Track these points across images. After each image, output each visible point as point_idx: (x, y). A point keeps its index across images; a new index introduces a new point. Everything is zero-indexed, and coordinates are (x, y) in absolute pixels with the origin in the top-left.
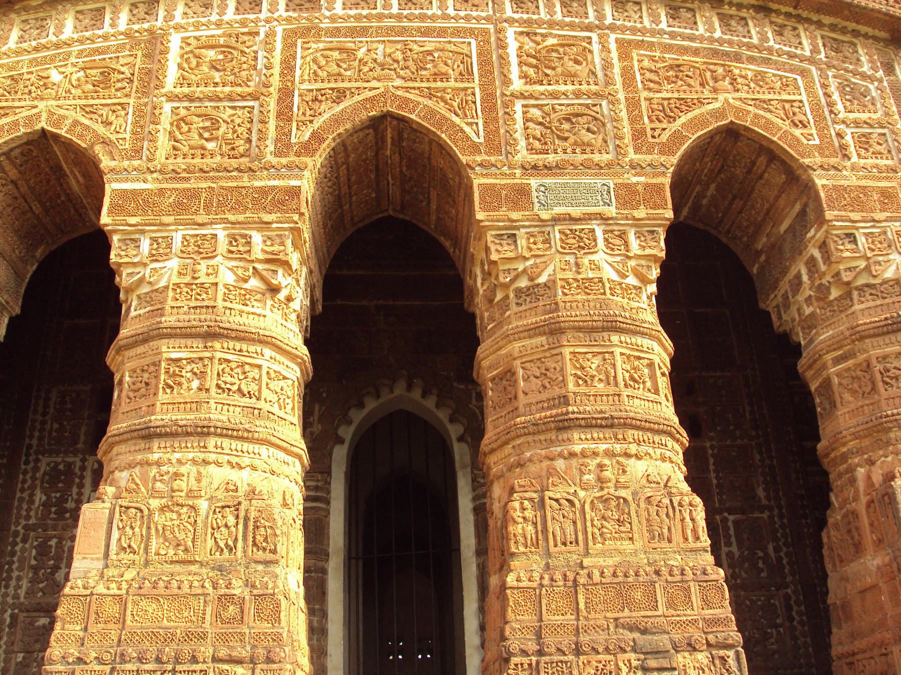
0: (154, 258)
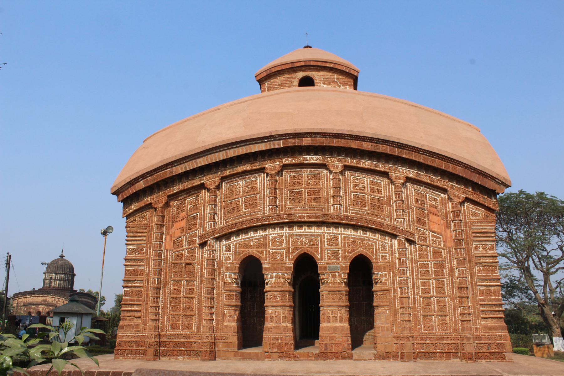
0: (271, 278)
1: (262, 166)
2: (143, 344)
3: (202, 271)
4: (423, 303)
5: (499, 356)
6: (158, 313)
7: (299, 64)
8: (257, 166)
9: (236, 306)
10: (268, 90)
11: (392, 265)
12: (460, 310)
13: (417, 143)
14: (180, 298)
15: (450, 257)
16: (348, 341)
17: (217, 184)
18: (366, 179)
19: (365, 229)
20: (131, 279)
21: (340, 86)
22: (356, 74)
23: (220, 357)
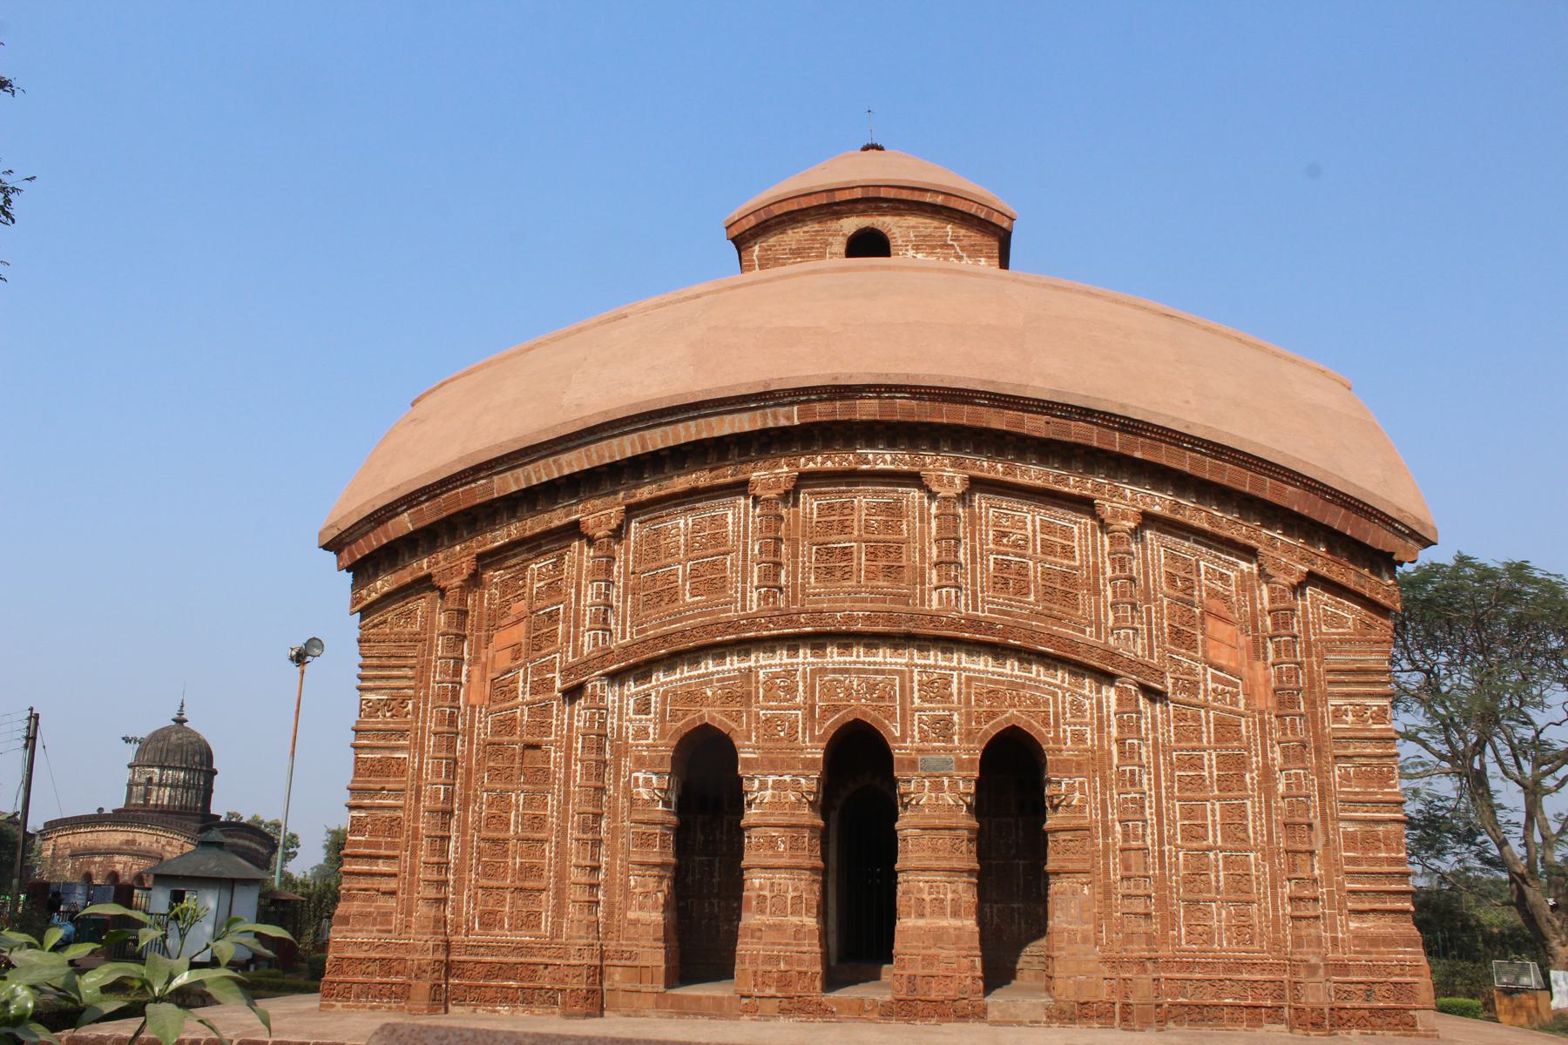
0: (760, 789)
1: (741, 477)
2: (400, 968)
3: (568, 766)
4: (1186, 867)
5: (1398, 1018)
6: (445, 883)
7: (847, 196)
8: (727, 475)
9: (662, 865)
10: (762, 267)
11: (1101, 759)
12: (1288, 889)
13: (1174, 419)
14: (505, 840)
15: (1263, 737)
16: (973, 968)
17: (614, 524)
18: (1029, 517)
19: (1026, 655)
20: (371, 786)
21: (960, 258)
22: (1005, 225)
23: (616, 1008)
